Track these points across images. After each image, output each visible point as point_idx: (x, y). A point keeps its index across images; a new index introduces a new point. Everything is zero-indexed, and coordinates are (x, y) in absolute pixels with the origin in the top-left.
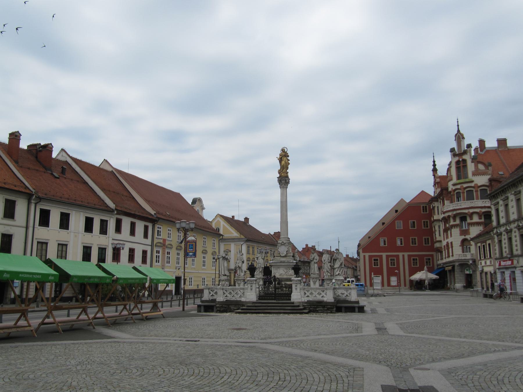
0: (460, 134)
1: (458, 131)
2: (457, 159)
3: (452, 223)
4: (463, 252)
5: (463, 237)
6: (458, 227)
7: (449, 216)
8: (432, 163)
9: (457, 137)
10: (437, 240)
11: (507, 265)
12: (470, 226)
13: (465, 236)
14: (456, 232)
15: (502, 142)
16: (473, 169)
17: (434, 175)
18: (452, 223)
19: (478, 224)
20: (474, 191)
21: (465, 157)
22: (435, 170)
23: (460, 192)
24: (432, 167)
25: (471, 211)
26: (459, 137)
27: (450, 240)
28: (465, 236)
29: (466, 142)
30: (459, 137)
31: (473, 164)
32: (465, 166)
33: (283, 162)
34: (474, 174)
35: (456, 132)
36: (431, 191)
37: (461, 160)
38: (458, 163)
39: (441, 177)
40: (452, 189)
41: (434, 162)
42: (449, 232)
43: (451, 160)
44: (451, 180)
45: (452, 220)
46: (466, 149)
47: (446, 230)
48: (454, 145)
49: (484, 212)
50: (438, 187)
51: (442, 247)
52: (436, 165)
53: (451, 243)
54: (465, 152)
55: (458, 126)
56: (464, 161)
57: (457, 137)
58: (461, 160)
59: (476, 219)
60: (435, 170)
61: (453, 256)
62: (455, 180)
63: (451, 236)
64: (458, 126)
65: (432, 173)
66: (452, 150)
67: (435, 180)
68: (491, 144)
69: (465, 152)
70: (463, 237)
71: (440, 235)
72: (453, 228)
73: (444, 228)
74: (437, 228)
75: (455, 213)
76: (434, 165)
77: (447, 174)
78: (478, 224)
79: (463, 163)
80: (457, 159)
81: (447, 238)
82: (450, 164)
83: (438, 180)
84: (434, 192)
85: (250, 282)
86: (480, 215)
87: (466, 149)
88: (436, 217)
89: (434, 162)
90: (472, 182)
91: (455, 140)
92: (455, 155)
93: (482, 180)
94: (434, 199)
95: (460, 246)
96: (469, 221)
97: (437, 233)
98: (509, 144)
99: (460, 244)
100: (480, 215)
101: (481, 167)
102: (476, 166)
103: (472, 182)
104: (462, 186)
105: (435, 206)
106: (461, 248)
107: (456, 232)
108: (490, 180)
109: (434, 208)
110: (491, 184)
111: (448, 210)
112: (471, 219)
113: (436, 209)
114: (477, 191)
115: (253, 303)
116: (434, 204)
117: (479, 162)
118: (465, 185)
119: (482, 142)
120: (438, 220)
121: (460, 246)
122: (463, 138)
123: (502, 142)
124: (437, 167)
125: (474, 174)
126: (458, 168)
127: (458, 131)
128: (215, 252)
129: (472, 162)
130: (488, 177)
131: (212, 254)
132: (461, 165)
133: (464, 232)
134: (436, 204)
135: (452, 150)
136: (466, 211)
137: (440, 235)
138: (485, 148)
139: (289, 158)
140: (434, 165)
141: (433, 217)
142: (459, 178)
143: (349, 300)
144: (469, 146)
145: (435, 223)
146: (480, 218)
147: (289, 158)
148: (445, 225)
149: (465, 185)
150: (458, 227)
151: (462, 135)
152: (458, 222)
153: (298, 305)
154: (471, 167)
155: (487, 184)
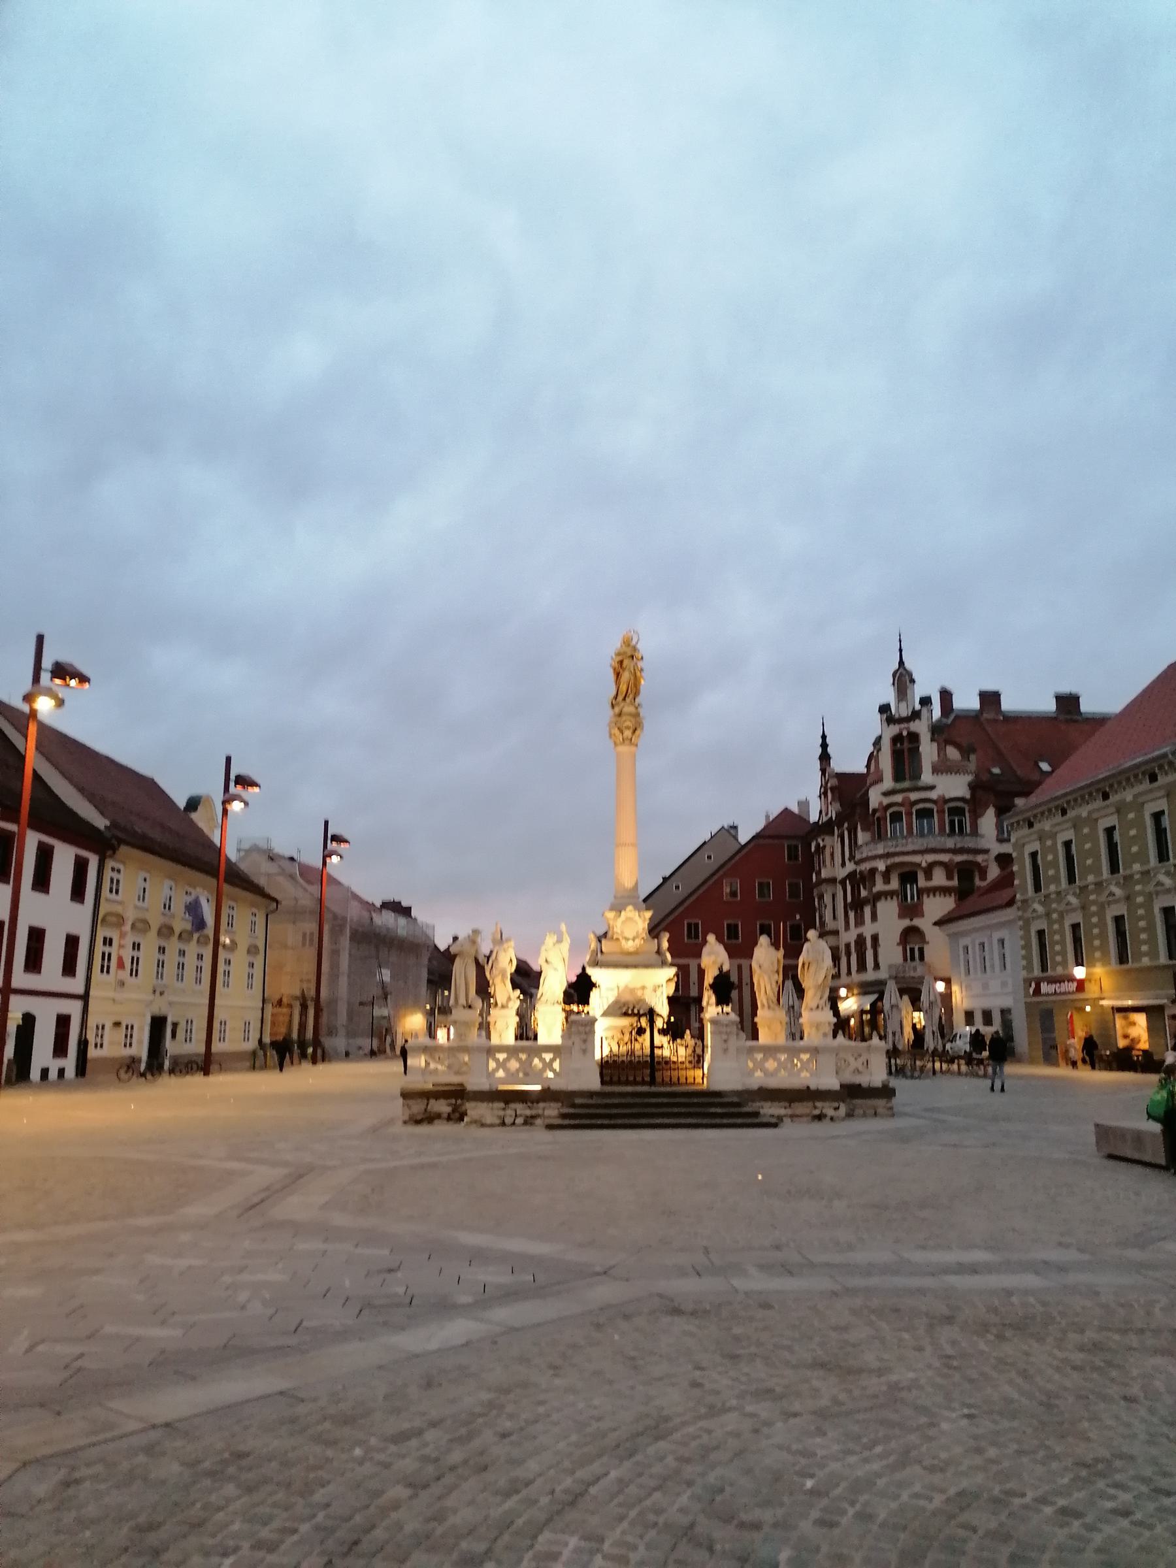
0: (905, 669)
1: (901, 663)
2: (894, 729)
3: (880, 886)
4: (905, 959)
5: (906, 923)
6: (895, 898)
7: (873, 871)
8: (820, 741)
9: (896, 679)
11: (1061, 994)
12: (925, 896)
13: (911, 920)
14: (888, 909)
15: (990, 699)
16: (936, 758)
17: (823, 771)
18: (880, 886)
19: (944, 891)
20: (935, 810)
21: (915, 726)
22: (825, 757)
23: (900, 813)
24: (820, 750)
25: (931, 858)
26: (903, 679)
27: (868, 930)
28: (911, 920)
29: (919, 691)
30: (903, 679)
31: (935, 745)
32: (915, 751)
33: (626, 676)
34: (936, 770)
35: (897, 666)
37: (905, 733)
38: (897, 739)
39: (842, 777)
40: (881, 803)
41: (824, 737)
42: (867, 911)
43: (879, 732)
44: (880, 780)
45: (879, 879)
46: (918, 707)
47: (857, 905)
48: (888, 695)
49: (958, 863)
50: (833, 799)
51: (838, 948)
52: (827, 745)
53: (875, 938)
54: (916, 715)
55: (901, 650)
56: (914, 737)
57: (896, 679)
58: (905, 733)
59: (939, 878)
60: (825, 757)
61: (877, 966)
62: (888, 783)
63: (874, 917)
64: (901, 650)
65: (817, 765)
66: (884, 709)
68: (967, 701)
69: (916, 715)
70: (906, 923)
71: (834, 917)
72: (883, 898)
73: (849, 899)
74: (827, 899)
75: (890, 861)
76: (824, 745)
77: (868, 766)
78: (944, 891)
79: (910, 742)
80: (894, 729)
81: (860, 922)
82: (877, 742)
83: (833, 782)
84: (821, 812)
85: (581, 1029)
86: (948, 868)
87: (918, 707)
89: (824, 737)
90: (932, 788)
91: (894, 684)
92: (891, 720)
93: (955, 786)
94: (825, 828)
95: (898, 944)
96: (922, 882)
98: (1007, 705)
99: (898, 941)
100: (948, 868)
101: (953, 753)
102: (941, 751)
103: (932, 788)
104: (909, 798)
105: (824, 847)
106: (900, 948)
107: (888, 909)
108: (973, 787)
109: (820, 850)
110: (973, 795)
111: (870, 854)
112: (928, 875)
113: (828, 852)
114: (940, 812)
115: (591, 1094)
116: (823, 840)
117: (948, 742)
118: (914, 796)
119: (946, 696)
120: (832, 881)
121: (898, 944)
122: (913, 681)
123: (990, 699)
125: (936, 770)
126: (897, 756)
127: (901, 663)
128: (256, 947)
129: (932, 740)
130: (969, 778)
131: (249, 952)
132: (906, 745)
133: (911, 910)
134: (831, 843)
135: (884, 709)
136: (916, 859)
137: (834, 917)
138: (952, 709)
139: (640, 664)
140: (824, 745)
141: (819, 873)
142: (898, 776)
143: (865, 1084)
144: (926, 701)
145: (824, 887)
146: (949, 877)
147: (640, 664)
149: (914, 796)
150: (895, 898)
151: (910, 674)
152: (895, 884)
153: (735, 1099)
154: (928, 751)
155: (968, 796)
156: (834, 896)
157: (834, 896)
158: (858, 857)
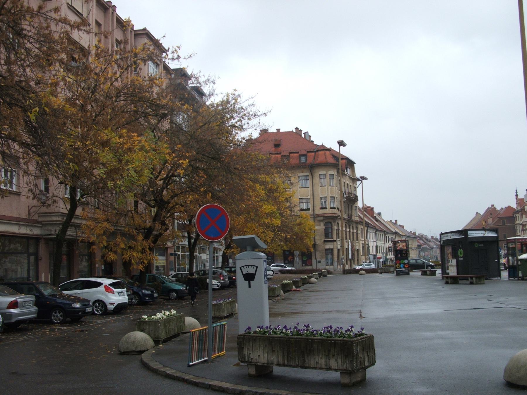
8: (515, 192)
10: (518, 234)
17: (516, 199)
22: (517, 195)
24: (515, 194)
36: (514, 206)
41: (516, 191)
42: (525, 232)
60: (517, 195)
65: (515, 197)
67: (517, 202)
76: (517, 193)
83: (519, 202)
88: (517, 222)
89: (516, 191)
97: (518, 231)
113: (518, 218)
120: (519, 224)
124: (518, 193)
140: (517, 193)
141: (516, 222)
148: (523, 228)
156: (519, 227)
157: (519, 227)
158: (523, 221)
